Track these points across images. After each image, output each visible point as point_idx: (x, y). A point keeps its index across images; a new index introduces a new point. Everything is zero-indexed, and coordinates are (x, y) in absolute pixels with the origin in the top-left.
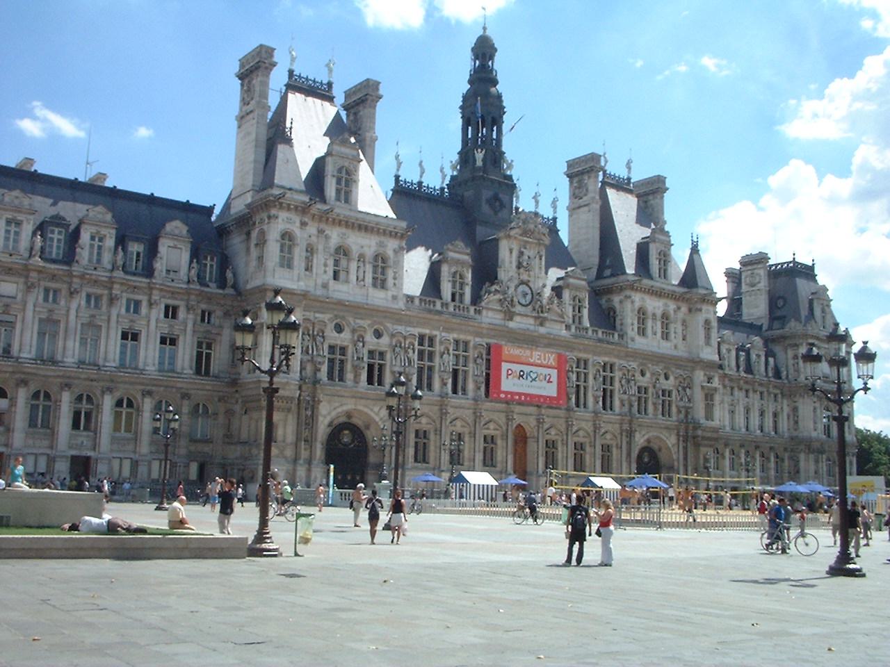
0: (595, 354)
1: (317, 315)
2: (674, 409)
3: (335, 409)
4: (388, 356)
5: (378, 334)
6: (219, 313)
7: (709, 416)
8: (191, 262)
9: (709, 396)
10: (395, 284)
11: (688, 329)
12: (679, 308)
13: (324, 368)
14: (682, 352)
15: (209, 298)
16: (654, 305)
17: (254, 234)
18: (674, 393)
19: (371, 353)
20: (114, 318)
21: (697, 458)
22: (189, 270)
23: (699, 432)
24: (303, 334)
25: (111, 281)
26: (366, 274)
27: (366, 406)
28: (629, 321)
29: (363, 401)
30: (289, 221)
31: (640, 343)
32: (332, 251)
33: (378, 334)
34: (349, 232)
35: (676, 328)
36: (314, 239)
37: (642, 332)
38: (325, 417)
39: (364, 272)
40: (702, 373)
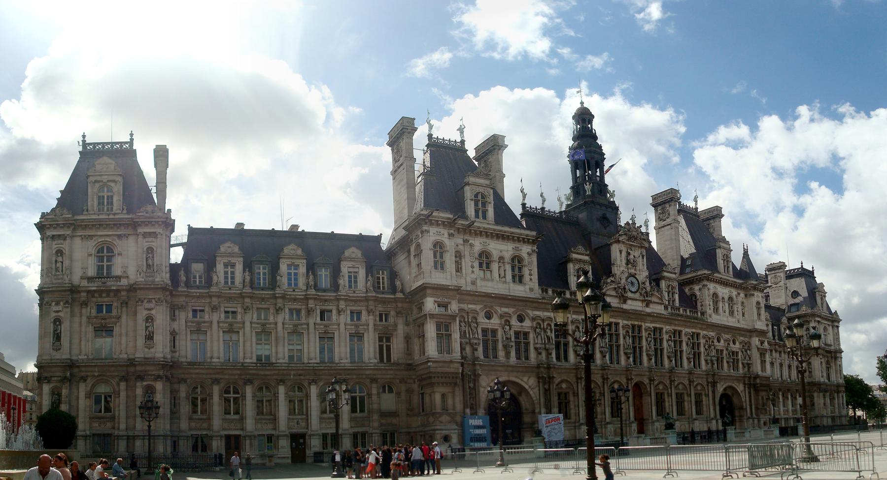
0: (686, 327)
1: (470, 306)
2: (740, 365)
4: (531, 336)
5: (521, 319)
6: (392, 313)
7: (763, 369)
8: (367, 276)
9: (762, 354)
11: (746, 309)
12: (739, 294)
13: (480, 349)
14: (743, 325)
15: (384, 302)
16: (724, 292)
17: (412, 249)
18: (740, 354)
19: (517, 334)
20: (312, 326)
21: (757, 400)
22: (366, 283)
23: (758, 381)
24: (460, 322)
25: (307, 298)
26: (507, 272)
27: (516, 377)
28: (707, 303)
31: (715, 319)
32: (476, 255)
33: (521, 319)
34: (489, 241)
35: (738, 308)
36: (461, 247)
37: (716, 310)
40: (757, 339)
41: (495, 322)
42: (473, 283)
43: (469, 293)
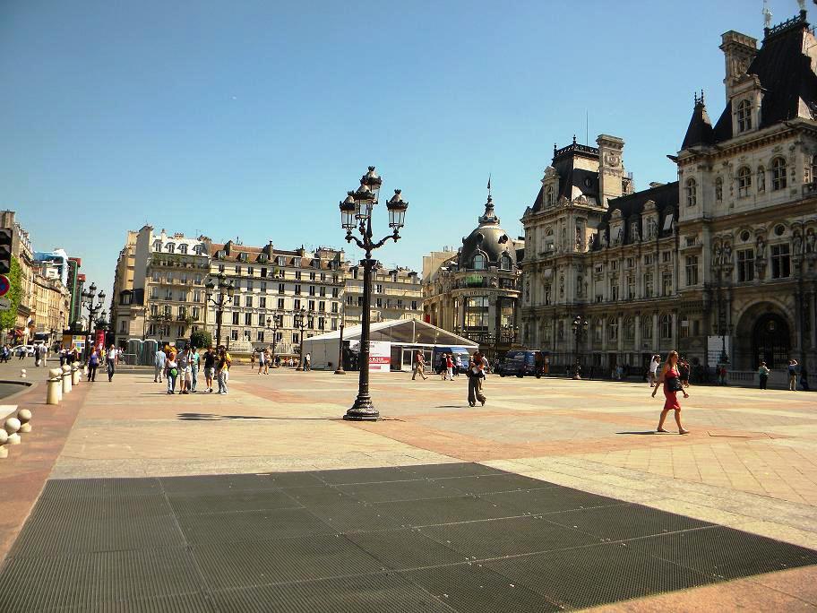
3: (746, 304)
10: (794, 180)
13: (736, 272)
26: (766, 182)
27: (772, 297)
29: (769, 294)
30: (690, 170)
33: (780, 231)
36: (721, 172)
38: (738, 312)
39: (764, 181)
41: (752, 240)
42: (732, 206)
43: (723, 219)
